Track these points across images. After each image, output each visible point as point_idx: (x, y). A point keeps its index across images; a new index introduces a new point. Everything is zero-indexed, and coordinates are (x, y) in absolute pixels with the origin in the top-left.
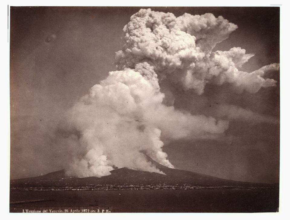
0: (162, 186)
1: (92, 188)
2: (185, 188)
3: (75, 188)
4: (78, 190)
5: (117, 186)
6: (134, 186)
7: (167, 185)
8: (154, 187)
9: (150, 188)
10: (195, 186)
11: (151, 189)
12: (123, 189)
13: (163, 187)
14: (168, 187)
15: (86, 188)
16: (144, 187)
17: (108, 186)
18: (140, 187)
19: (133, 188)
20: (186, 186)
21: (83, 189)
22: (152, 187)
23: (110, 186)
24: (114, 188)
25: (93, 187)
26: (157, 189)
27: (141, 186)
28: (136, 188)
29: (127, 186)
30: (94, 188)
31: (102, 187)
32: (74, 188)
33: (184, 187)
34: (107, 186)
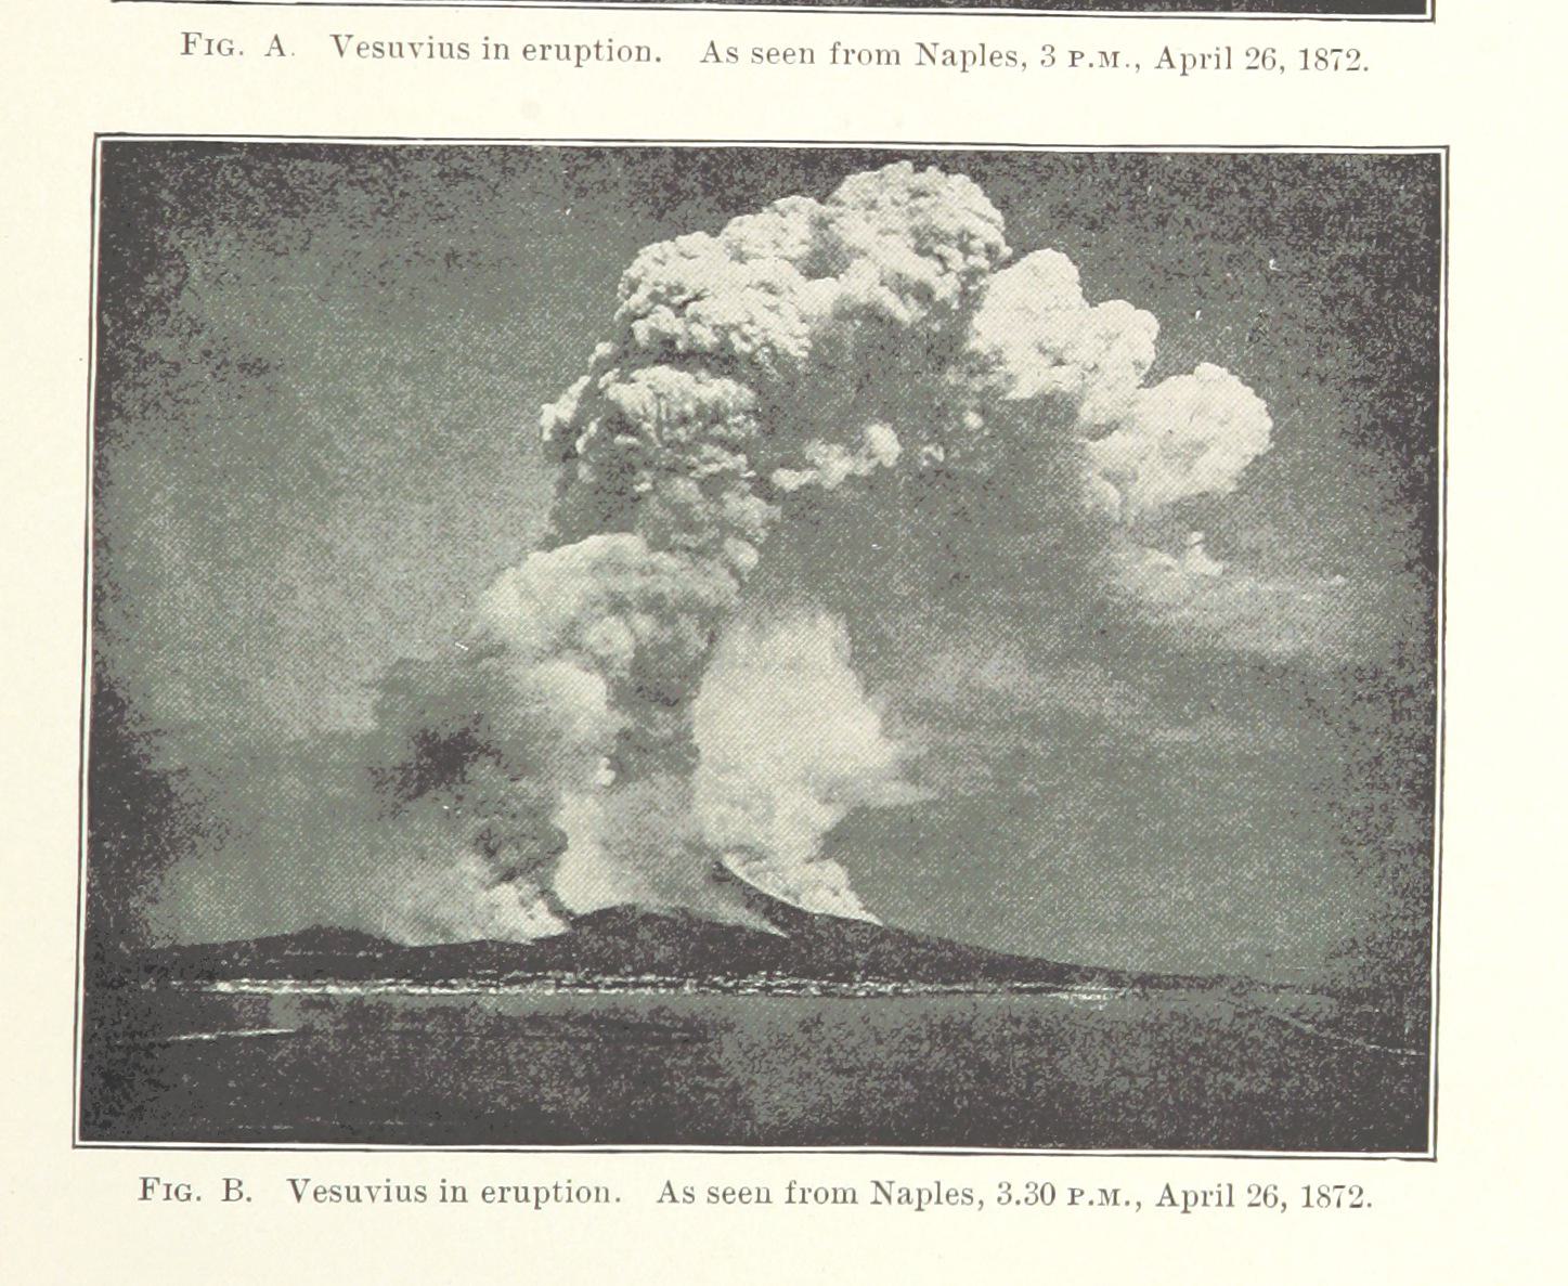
0: (770, 977)
1: (490, 985)
2: (861, 988)
3: (423, 985)
4: (435, 990)
5: (589, 979)
6: (661, 978)
7: (794, 975)
8: (736, 987)
9: (720, 987)
10: (894, 979)
11: (726, 990)
12: (613, 991)
13: (773, 984)
14: (792, 986)
15: (469, 985)
16: (698, 986)
17: (556, 979)
18: (682, 984)
19: (654, 985)
20: (864, 979)
21: (452, 987)
22: (731, 984)
23: (564, 978)
24: (582, 984)
25: (495, 983)
26: (750, 991)
27: (688, 977)
28: (668, 985)
29: (632, 979)
30: (497, 987)
31: (529, 981)
32: (419, 982)
33: (856, 986)
34: (549, 978)
